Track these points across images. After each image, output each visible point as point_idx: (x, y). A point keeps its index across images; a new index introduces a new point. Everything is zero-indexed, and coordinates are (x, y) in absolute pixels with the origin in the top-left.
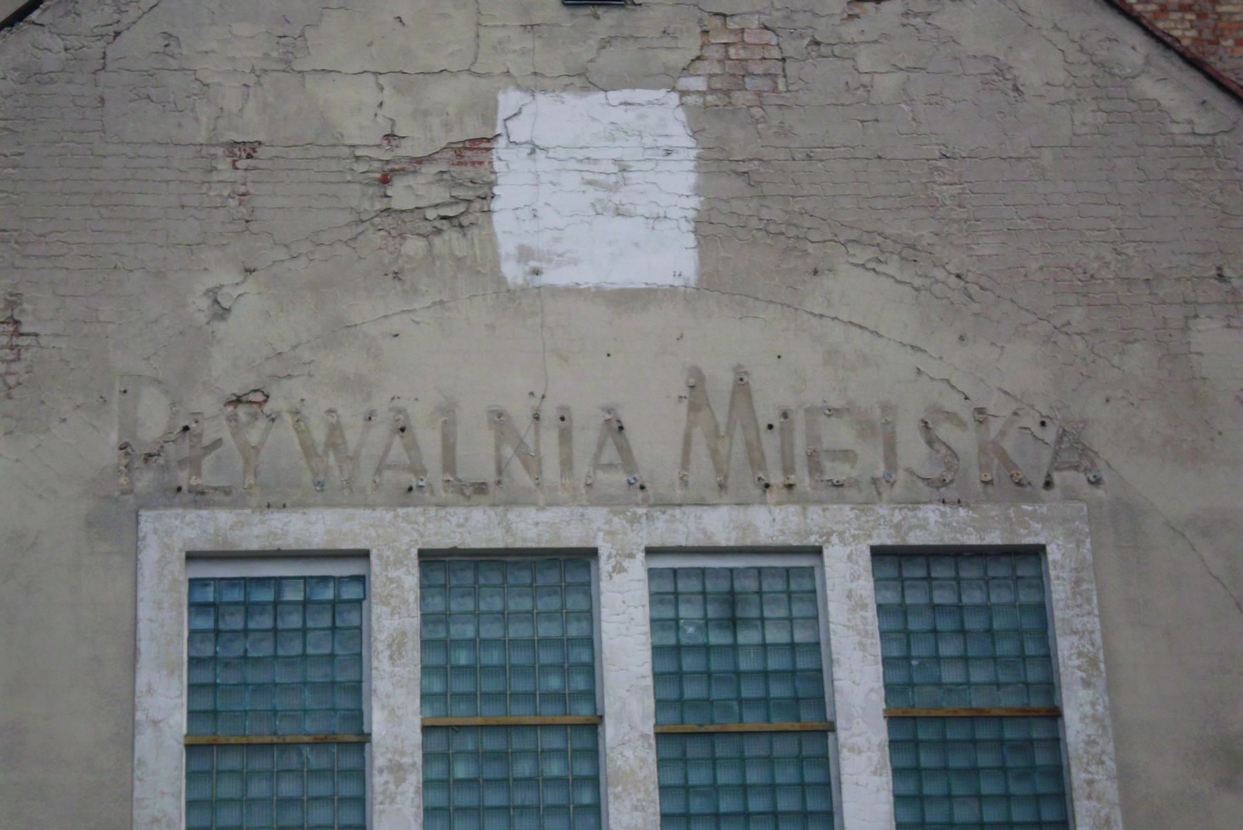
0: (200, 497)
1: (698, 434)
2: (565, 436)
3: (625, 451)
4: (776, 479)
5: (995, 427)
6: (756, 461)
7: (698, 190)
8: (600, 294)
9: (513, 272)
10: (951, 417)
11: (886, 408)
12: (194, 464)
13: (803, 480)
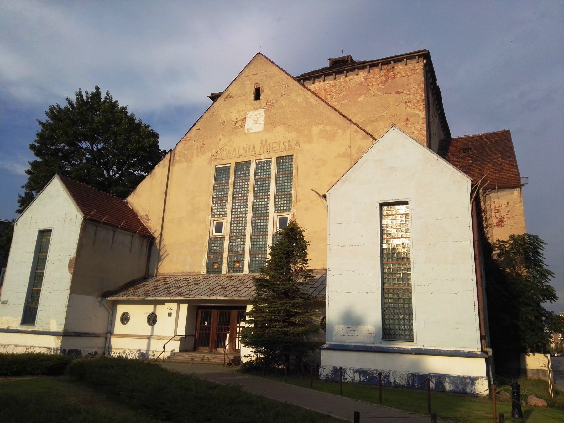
1: (262, 147)
2: (249, 149)
3: (255, 150)
4: (268, 151)
5: (290, 142)
6: (267, 149)
7: (264, 120)
8: (254, 133)
9: (246, 132)
10: (286, 142)
11: (280, 141)
12: (216, 156)
13: (271, 150)
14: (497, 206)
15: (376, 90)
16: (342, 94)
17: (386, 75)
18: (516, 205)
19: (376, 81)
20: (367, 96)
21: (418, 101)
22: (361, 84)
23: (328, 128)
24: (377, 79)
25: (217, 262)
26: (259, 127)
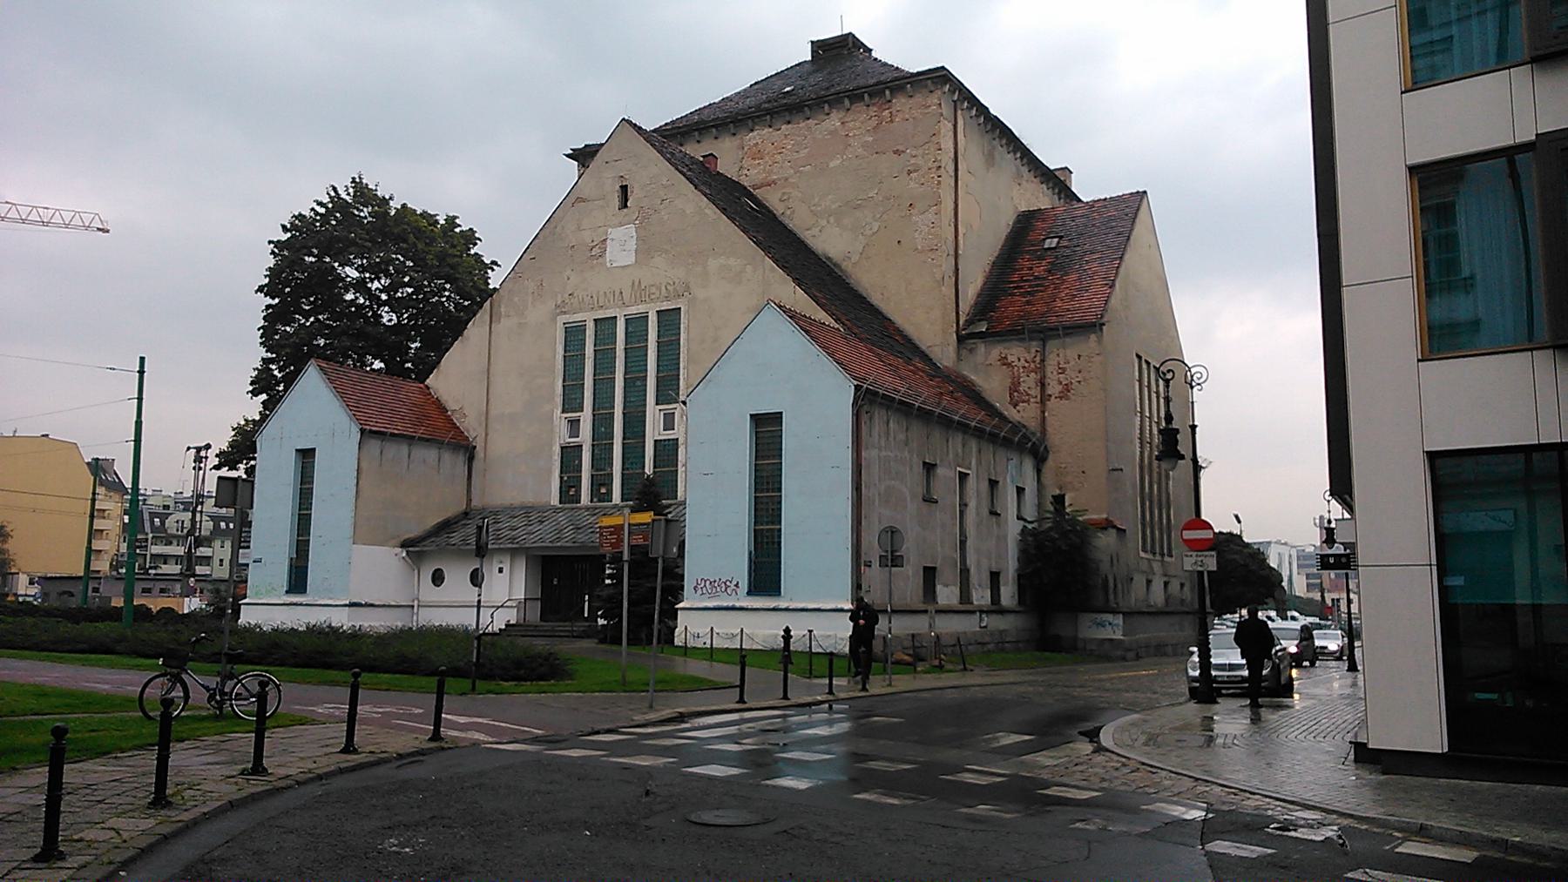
0: (565, 313)
2: (614, 295)
3: (622, 297)
6: (641, 297)
9: (608, 265)
14: (1062, 363)
15: (859, 146)
16: (804, 153)
17: (875, 116)
18: (1092, 360)
19: (860, 128)
20: (845, 157)
21: (929, 169)
22: (833, 133)
23: (732, 261)
24: (862, 123)
25: (573, 487)
26: (631, 259)
